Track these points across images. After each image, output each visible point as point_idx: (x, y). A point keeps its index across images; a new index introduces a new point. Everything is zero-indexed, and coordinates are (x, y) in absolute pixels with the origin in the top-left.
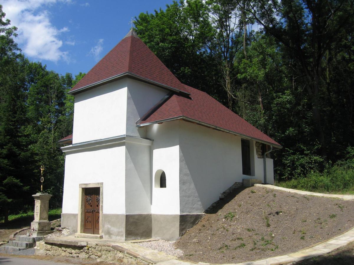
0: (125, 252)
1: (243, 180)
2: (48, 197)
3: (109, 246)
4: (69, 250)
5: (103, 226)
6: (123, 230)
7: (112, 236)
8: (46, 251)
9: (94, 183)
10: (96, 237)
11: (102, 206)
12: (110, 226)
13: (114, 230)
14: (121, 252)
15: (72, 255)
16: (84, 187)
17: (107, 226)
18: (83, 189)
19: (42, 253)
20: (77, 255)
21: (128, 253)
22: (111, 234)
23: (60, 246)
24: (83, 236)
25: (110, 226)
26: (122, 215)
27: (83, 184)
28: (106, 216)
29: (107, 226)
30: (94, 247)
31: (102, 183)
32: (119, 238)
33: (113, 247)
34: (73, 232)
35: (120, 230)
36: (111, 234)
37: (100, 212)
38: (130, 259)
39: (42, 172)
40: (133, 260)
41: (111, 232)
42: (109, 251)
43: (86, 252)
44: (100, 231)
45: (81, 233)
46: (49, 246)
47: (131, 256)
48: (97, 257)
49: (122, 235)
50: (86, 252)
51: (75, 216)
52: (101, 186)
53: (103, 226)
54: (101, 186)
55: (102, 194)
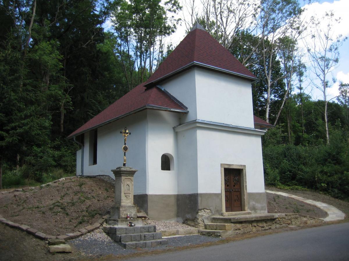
4: (260, 225)
5: (248, 203)
7: (257, 211)
8: (234, 231)
9: (237, 165)
11: (246, 186)
12: (254, 203)
13: (258, 205)
15: (264, 229)
16: (226, 167)
17: (252, 203)
18: (226, 170)
19: (230, 234)
20: (270, 227)
23: (241, 222)
24: (234, 214)
27: (226, 164)
28: (251, 195)
29: (252, 203)
32: (263, 211)
34: (216, 212)
35: (263, 206)
37: (245, 191)
38: (311, 221)
40: (313, 221)
41: (256, 208)
42: (296, 218)
44: (246, 208)
46: (239, 226)
47: (312, 219)
49: (265, 209)
51: (217, 195)
52: (244, 168)
53: (249, 203)
54: (244, 168)
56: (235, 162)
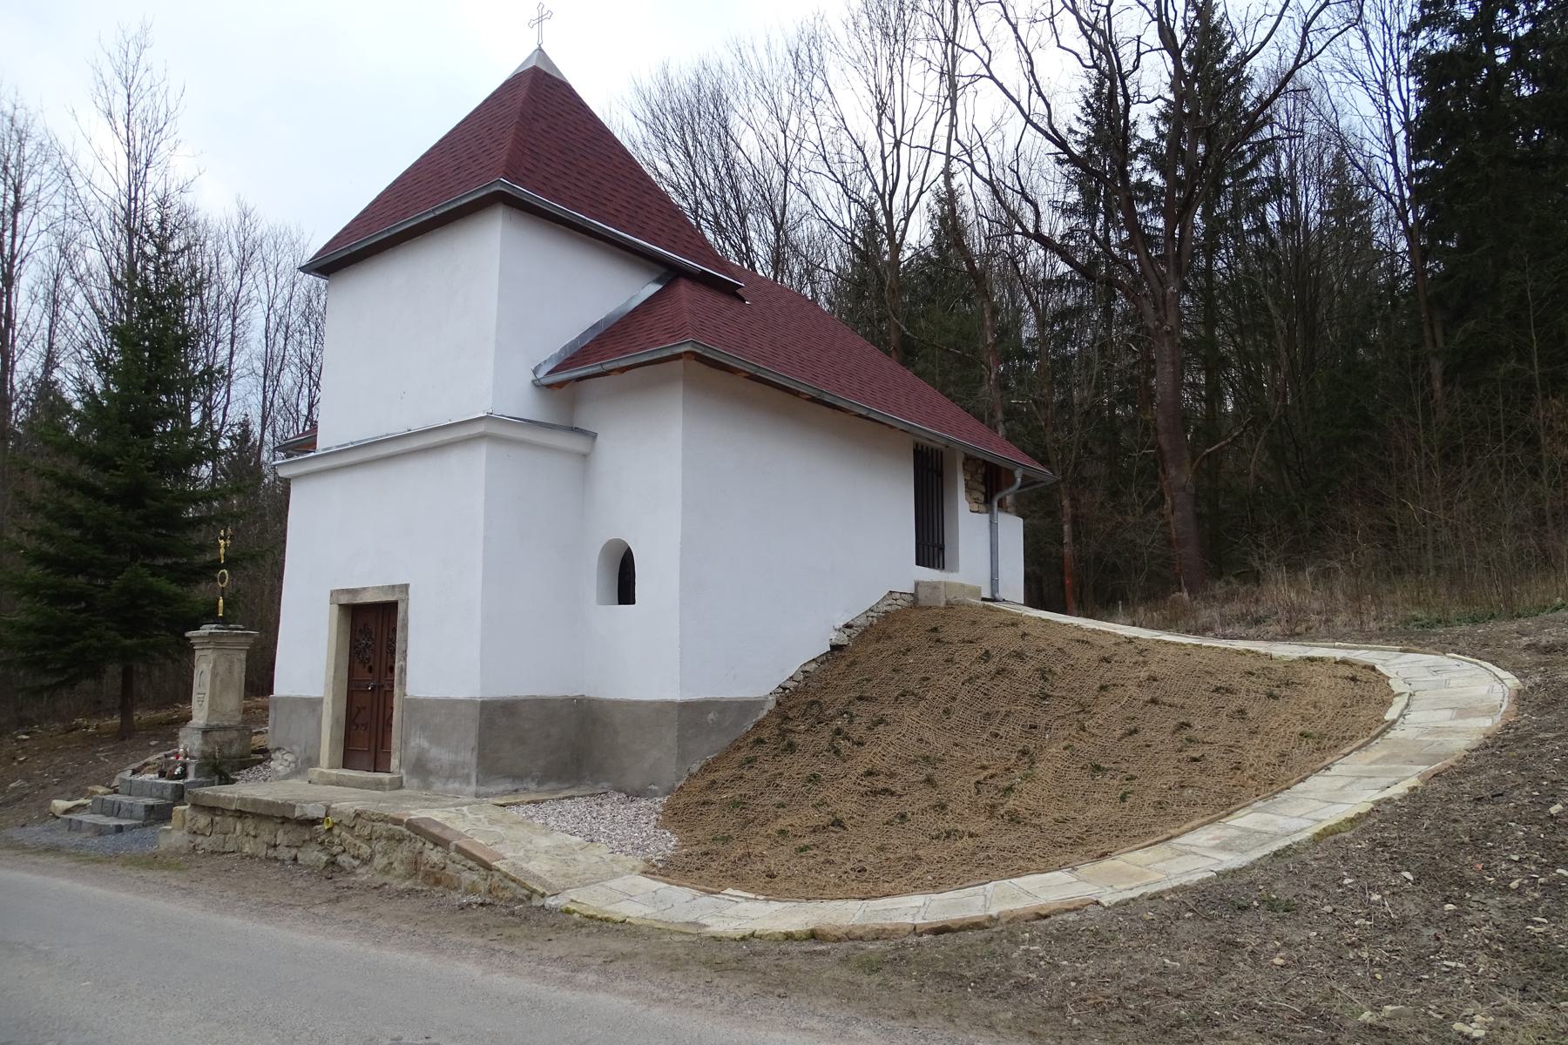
0: (452, 847)
1: (917, 584)
2: (243, 640)
3: (398, 822)
5: (406, 741)
6: (469, 757)
7: (432, 779)
10: (379, 785)
11: (403, 670)
12: (426, 744)
14: (436, 845)
16: (344, 600)
17: (418, 742)
18: (343, 607)
20: (294, 851)
21: (459, 850)
22: (430, 773)
25: (426, 744)
26: (469, 702)
29: (418, 742)
30: (346, 822)
31: (407, 586)
33: (410, 825)
35: (460, 759)
36: (430, 773)
39: (222, 551)
41: (431, 766)
43: (322, 843)
44: (394, 762)
45: (331, 767)
47: (471, 864)
48: (356, 863)
50: (322, 843)
51: (314, 704)
53: (404, 742)
55: (405, 626)
56: (370, 581)
